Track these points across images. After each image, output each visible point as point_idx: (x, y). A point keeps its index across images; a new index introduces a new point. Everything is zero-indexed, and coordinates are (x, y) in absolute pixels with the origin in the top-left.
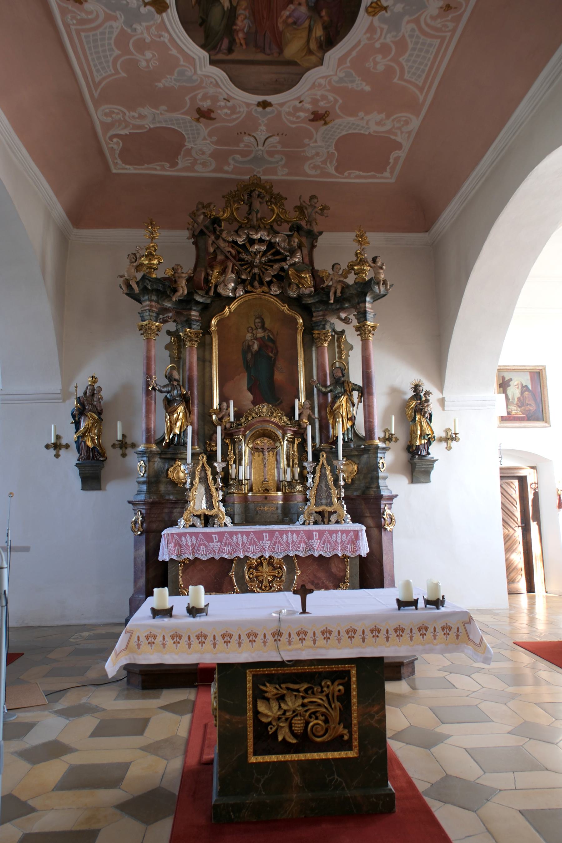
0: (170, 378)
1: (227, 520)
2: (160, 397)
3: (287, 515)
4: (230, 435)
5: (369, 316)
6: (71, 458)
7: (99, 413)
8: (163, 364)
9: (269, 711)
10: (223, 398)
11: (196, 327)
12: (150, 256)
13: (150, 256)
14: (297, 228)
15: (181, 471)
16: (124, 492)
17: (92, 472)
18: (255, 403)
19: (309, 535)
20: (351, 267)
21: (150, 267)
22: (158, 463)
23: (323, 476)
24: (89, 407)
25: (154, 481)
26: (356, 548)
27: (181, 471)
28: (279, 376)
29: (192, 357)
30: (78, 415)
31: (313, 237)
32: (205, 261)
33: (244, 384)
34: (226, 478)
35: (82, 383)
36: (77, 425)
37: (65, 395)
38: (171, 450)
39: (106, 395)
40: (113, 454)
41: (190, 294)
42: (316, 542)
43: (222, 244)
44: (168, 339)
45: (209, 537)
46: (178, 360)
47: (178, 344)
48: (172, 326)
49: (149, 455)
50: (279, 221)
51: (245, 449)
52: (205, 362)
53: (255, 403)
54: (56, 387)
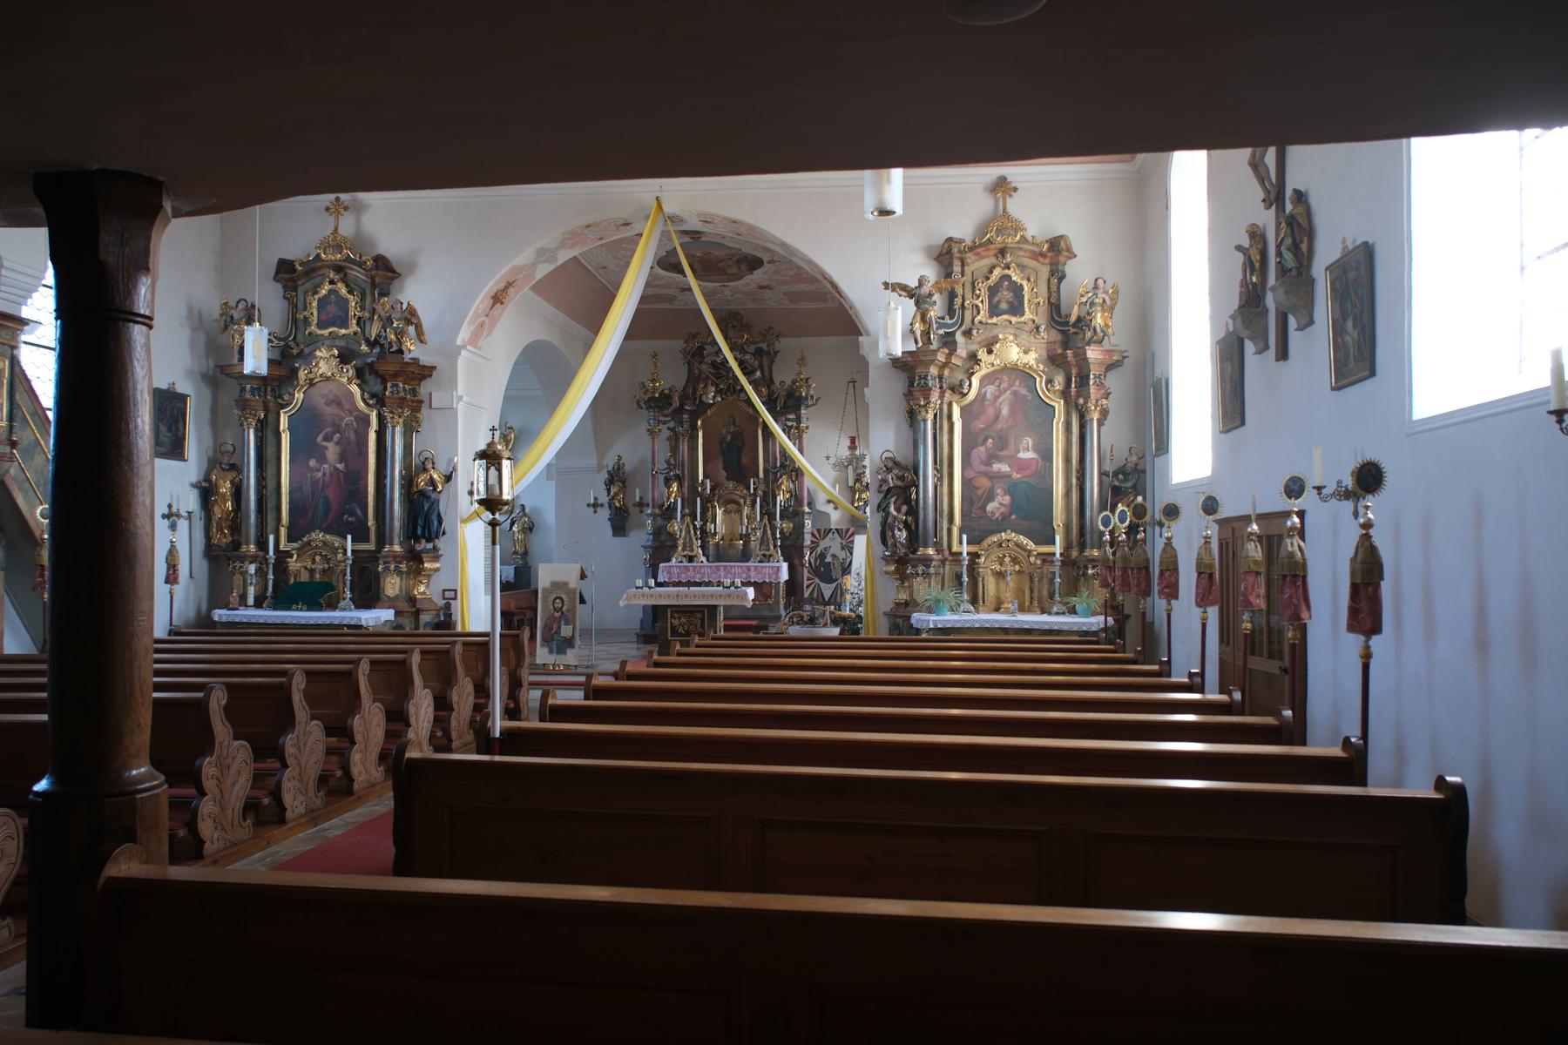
0: (668, 462)
1: (704, 559)
2: (661, 478)
3: (745, 556)
4: (707, 502)
5: (803, 419)
6: (605, 513)
7: (624, 482)
8: (664, 453)
9: (676, 622)
10: (705, 476)
11: (686, 426)
12: (654, 381)
13: (654, 381)
14: (759, 353)
15: (675, 526)
16: (640, 538)
17: (620, 524)
18: (728, 479)
19: (749, 568)
20: (794, 382)
21: (654, 388)
22: (660, 521)
23: (765, 532)
24: (616, 477)
25: (657, 533)
26: (777, 577)
27: (675, 526)
28: (744, 460)
29: (684, 447)
30: (610, 483)
31: (772, 355)
32: (693, 380)
33: (721, 466)
34: (703, 531)
35: (610, 461)
36: (609, 491)
37: (600, 468)
38: (668, 513)
39: (628, 468)
40: (633, 511)
41: (682, 405)
42: (752, 573)
43: (704, 367)
44: (668, 433)
45: (687, 568)
46: (674, 450)
47: (675, 438)
48: (672, 425)
49: (654, 516)
50: (749, 342)
51: (719, 512)
52: (693, 449)
53: (728, 479)
54: (593, 462)
